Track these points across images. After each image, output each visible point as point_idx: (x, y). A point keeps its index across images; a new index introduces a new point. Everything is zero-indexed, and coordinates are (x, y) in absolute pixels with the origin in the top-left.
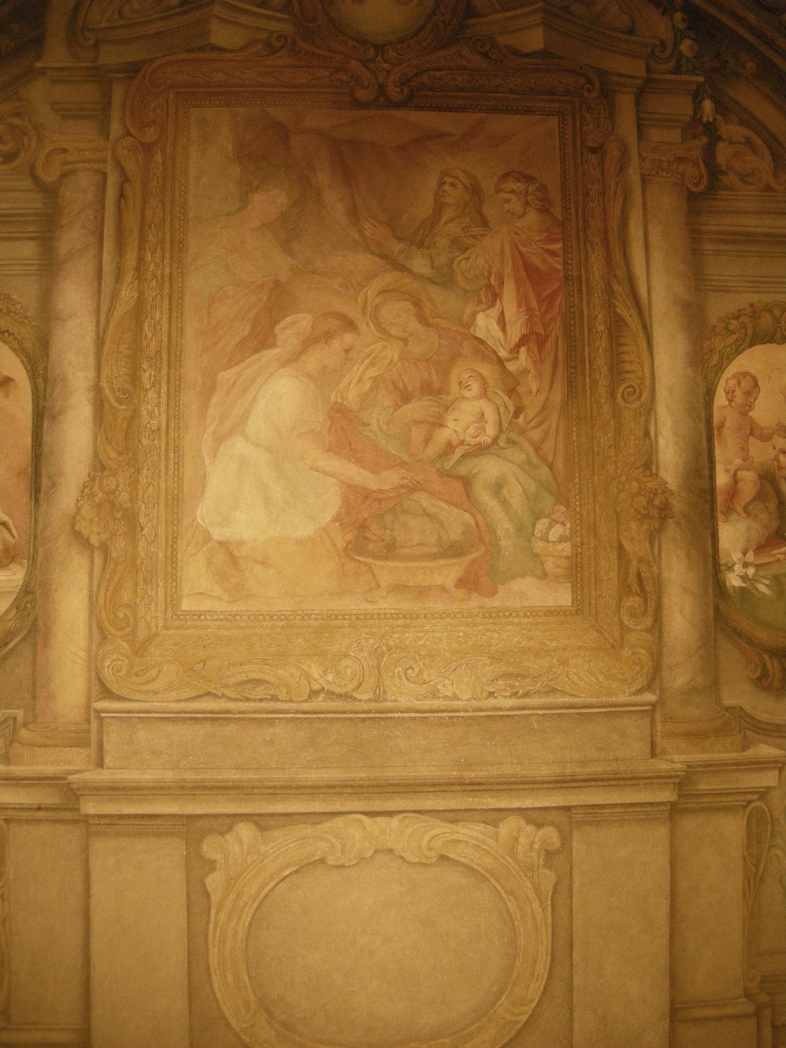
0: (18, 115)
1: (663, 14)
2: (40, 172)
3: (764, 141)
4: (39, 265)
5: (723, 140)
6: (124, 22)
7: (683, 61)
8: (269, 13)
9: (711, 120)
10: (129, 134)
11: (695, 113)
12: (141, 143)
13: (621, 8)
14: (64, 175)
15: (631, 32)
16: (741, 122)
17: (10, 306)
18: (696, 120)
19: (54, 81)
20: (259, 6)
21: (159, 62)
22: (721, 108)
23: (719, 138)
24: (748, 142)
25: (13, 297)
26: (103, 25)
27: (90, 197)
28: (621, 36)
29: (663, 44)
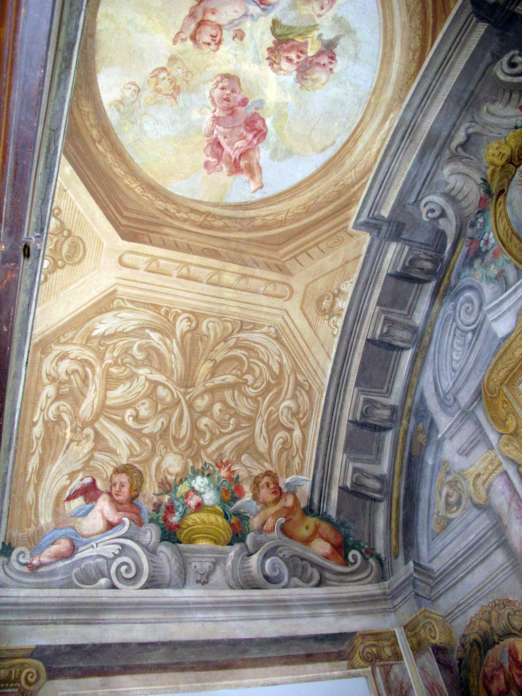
0: (448, 473)
2: (476, 500)
4: (510, 565)
6: (458, 373)
8: (514, 287)
10: (502, 434)
12: (510, 434)
14: (488, 491)
17: (512, 607)
19: (451, 438)
20: (506, 291)
21: (486, 377)
25: (511, 599)
26: (451, 385)
27: (507, 493)
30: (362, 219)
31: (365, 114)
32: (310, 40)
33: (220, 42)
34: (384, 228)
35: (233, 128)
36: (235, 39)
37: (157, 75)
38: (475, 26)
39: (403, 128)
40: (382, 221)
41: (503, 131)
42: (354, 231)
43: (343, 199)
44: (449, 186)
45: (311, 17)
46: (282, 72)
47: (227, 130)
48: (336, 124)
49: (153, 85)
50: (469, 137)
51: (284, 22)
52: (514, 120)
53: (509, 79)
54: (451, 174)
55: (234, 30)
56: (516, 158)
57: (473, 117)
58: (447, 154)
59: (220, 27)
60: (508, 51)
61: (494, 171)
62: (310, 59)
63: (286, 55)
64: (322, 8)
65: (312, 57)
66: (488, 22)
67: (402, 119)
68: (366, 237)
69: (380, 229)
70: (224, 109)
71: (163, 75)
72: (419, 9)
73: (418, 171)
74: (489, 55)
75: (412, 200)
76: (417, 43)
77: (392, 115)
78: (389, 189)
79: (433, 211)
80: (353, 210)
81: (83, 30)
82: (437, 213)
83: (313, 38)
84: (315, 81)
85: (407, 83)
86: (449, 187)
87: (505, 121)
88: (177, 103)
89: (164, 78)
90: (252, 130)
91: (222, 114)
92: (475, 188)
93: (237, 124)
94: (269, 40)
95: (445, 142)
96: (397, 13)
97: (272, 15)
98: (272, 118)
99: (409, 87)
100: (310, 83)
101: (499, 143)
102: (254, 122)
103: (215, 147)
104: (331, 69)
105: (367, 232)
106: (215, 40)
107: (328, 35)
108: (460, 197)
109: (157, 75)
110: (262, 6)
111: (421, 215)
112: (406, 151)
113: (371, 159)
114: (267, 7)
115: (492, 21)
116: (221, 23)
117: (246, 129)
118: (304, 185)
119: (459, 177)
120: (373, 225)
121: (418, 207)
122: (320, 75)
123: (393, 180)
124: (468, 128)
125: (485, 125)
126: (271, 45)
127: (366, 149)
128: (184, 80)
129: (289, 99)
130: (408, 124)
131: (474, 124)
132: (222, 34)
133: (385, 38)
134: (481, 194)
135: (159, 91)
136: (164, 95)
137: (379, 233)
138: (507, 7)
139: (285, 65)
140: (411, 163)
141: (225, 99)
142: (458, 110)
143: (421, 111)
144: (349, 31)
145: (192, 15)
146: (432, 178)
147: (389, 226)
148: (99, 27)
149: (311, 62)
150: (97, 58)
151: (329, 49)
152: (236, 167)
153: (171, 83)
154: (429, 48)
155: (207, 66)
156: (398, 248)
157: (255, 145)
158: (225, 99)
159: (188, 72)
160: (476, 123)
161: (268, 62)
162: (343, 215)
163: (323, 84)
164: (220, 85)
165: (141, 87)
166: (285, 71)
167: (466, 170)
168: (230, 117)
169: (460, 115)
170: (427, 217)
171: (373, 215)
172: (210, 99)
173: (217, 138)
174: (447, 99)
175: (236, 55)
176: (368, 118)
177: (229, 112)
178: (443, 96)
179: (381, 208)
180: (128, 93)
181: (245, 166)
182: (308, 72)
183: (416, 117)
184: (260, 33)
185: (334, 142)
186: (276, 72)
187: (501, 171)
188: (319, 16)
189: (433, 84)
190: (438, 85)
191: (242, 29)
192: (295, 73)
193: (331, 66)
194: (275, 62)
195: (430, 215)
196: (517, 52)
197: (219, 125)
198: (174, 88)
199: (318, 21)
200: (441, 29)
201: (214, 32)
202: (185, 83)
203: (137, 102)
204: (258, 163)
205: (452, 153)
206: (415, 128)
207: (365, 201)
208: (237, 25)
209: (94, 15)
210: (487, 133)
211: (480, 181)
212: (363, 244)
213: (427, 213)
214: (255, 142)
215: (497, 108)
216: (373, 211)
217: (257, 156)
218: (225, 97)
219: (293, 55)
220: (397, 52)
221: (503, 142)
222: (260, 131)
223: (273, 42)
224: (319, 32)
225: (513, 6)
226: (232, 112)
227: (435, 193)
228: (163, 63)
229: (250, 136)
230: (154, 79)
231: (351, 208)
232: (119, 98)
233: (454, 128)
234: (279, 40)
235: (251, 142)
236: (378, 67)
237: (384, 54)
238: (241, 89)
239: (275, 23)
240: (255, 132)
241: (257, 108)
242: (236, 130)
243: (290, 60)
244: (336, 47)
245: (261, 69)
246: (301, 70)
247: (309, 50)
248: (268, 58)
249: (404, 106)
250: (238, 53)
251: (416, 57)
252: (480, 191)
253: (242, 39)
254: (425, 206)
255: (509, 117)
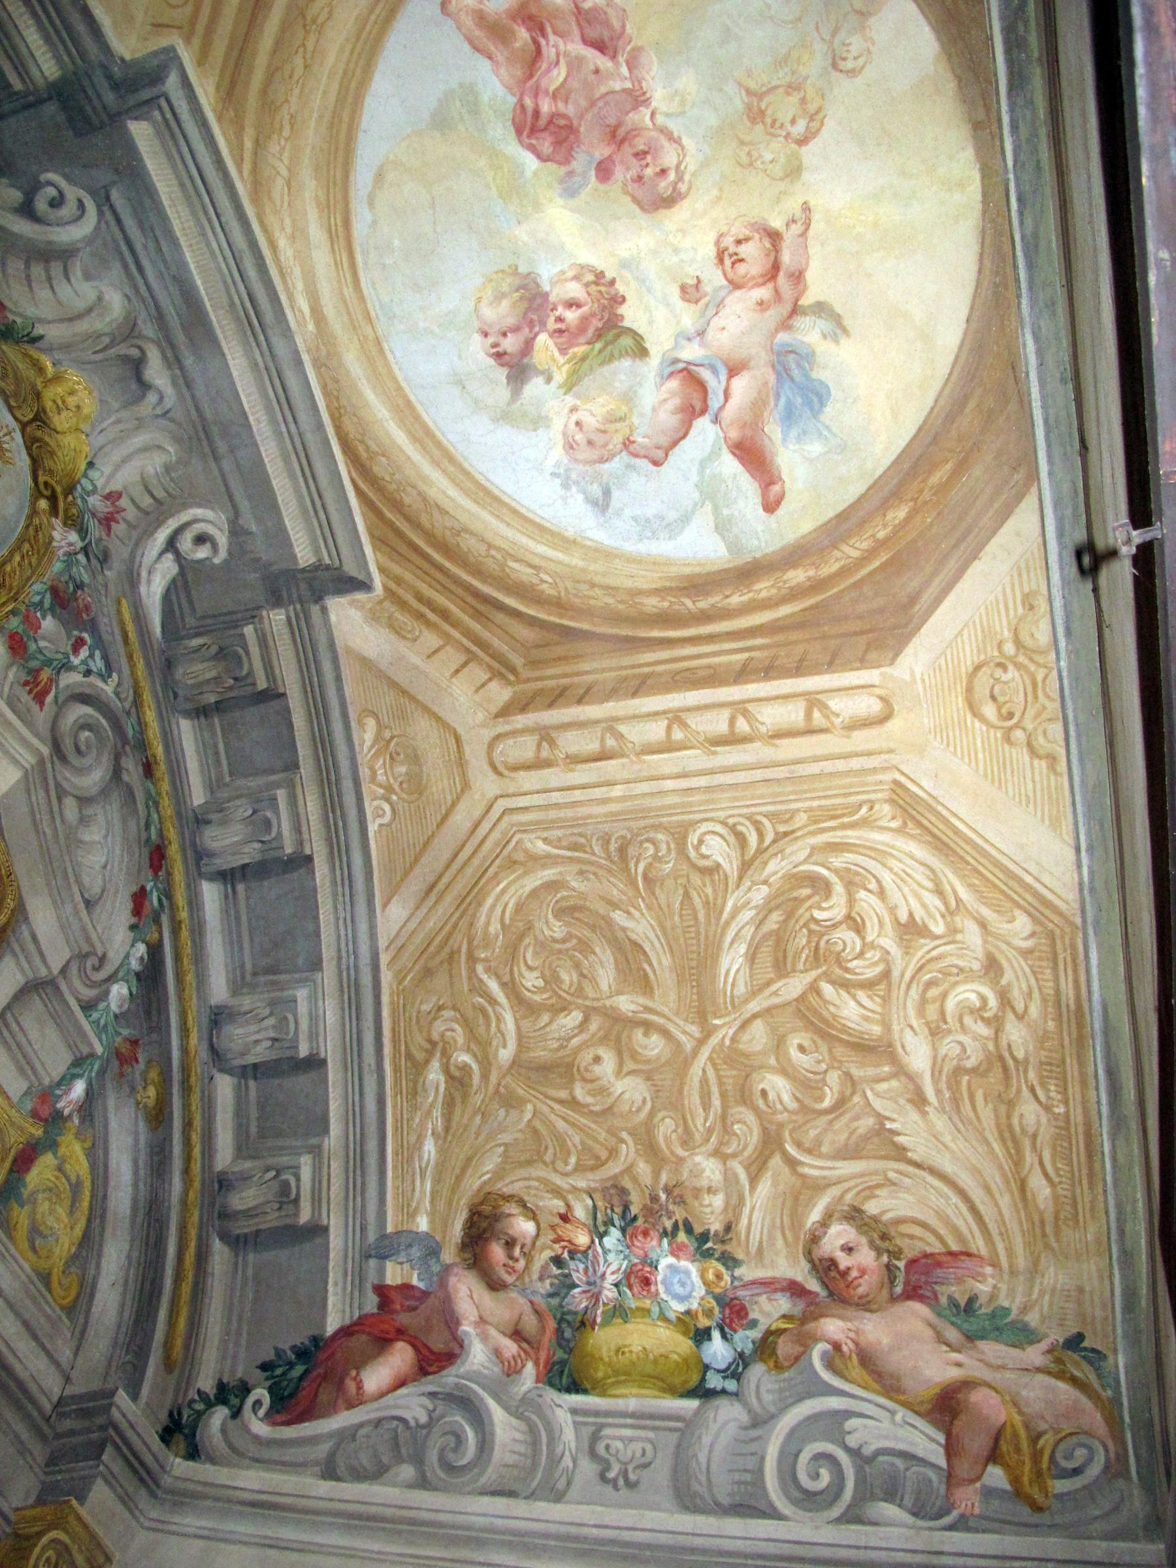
1: (133, 928)
3: (91, 1209)
5: (55, 1154)
7: (102, 1006)
9: (66, 1112)
11: (59, 1084)
13: (105, 867)
15: (88, 904)
16: (90, 1153)
18: (46, 1096)
22: (88, 1108)
23: (53, 1145)
24: (76, 1188)
28: (78, 898)
29: (103, 959)
30: (172, 81)
31: (362, 299)
32: (561, 360)
33: (720, 260)
34: (109, 97)
35: (593, 103)
36: (695, 281)
37: (812, 119)
38: (317, 550)
39: (269, 317)
40: (129, 109)
41: (101, 440)
42: (163, 42)
43: (253, 100)
44: (79, 273)
45: (587, 399)
46: (570, 274)
47: (603, 89)
48: (396, 242)
49: (810, 93)
50: (145, 386)
51: (626, 363)
52: (107, 470)
53: (185, 517)
54: (100, 299)
55: (706, 295)
56: (39, 434)
57: (172, 420)
58: (148, 329)
59: (735, 285)
60: (230, 553)
61: (41, 370)
62: (537, 329)
63: (585, 309)
64: (577, 424)
65: (536, 335)
66: (303, 570)
67: (287, 333)
68: (127, 45)
69: (116, 86)
70: (636, 131)
71: (800, 128)
72: (424, 519)
73: (165, 261)
74: (254, 528)
75: (115, 194)
76: (380, 468)
77: (311, 327)
78: (182, 185)
79: (57, 202)
80: (211, 89)
81: (1000, 128)
82: (41, 205)
83: (559, 368)
84: (500, 297)
85: (338, 398)
86: (77, 272)
87: (116, 457)
88: (740, 84)
89: (793, 122)
90: (550, 122)
91: (633, 118)
92: (31, 311)
93: (589, 116)
94: (632, 315)
95: (173, 347)
96: (452, 492)
97: (654, 361)
98: (529, 174)
99: (326, 394)
100: (505, 288)
101: (88, 417)
102: (558, 144)
103: (606, 35)
104: (486, 335)
105: (135, 62)
106: (731, 256)
107: (535, 387)
108: (37, 270)
109: (812, 119)
110: (681, 366)
111: (66, 177)
112: (225, 282)
113: (271, 219)
114: (670, 369)
115: (300, 576)
116: (738, 293)
117: (564, 116)
118: (358, 72)
119: (80, 305)
120: (142, 84)
121: (93, 193)
122: (500, 313)
123: (194, 213)
124: (161, 398)
125: (140, 424)
126: (623, 310)
127: (298, 234)
128: (751, 143)
129: (522, 234)
130: (270, 332)
131: (159, 411)
132: (725, 275)
133: (438, 444)
134: (14, 313)
135: (791, 88)
136: (776, 88)
137: (109, 77)
138: (298, 606)
139: (575, 290)
140: (192, 266)
141: (646, 153)
142: (208, 414)
143: (267, 369)
144: (504, 417)
145: (798, 277)
146: (125, 266)
147: (105, 108)
148: (969, 153)
149: (531, 324)
150: (951, 86)
151: (517, 367)
152: (531, 18)
153: (774, 121)
154: (354, 475)
155: (719, 198)
156: (34, 72)
157: (522, 95)
158: (646, 153)
159: (751, 164)
160: (157, 416)
161: (609, 275)
162: (220, 61)
163: (479, 300)
164: (672, 176)
165: (835, 75)
166: (566, 280)
167: (83, 326)
168: (612, 121)
169: (198, 409)
170: (50, 183)
171: (160, 108)
172: (676, 135)
173: (614, 57)
174: (247, 418)
175: (676, 251)
176: (348, 292)
177: (621, 132)
178: (258, 421)
179: (158, 133)
180: (856, 43)
181: (513, 32)
182: (525, 305)
183: (267, 353)
184: (656, 316)
185: (371, 204)
186: (582, 267)
187: (33, 386)
188: (574, 409)
189: (292, 427)
190: (284, 429)
191: (693, 307)
192: (546, 287)
193: (491, 340)
194: (596, 283)
195: (51, 192)
196: (217, 561)
197: (624, 90)
198: (762, 113)
199: (570, 400)
200: (363, 515)
201: (742, 269)
202: (747, 138)
203: (828, 38)
204: (490, 58)
205: (140, 336)
206: (249, 333)
207: (204, 125)
208: (707, 306)
209: (986, 173)
210: (124, 414)
211: (39, 330)
212: (115, 24)
213: (61, 194)
214: (528, 102)
215: (154, 464)
216: (169, 116)
217: (503, 71)
218: (649, 158)
219: (571, 316)
220: (400, 437)
221: (85, 427)
222: (534, 131)
223: (622, 317)
224: (554, 384)
225: (292, 614)
226: (617, 136)
227: (90, 240)
228: (809, 153)
229: (546, 107)
230: (812, 108)
231: (217, 89)
232: (872, 21)
233: (184, 381)
234: (616, 326)
235: (536, 96)
236: (407, 390)
237: (417, 418)
238: (627, 193)
239: (641, 351)
240: (542, 122)
241: (571, 174)
242: (584, 103)
243: (572, 304)
244: (509, 378)
245: (613, 255)
246: (539, 301)
247: (550, 342)
248: (612, 282)
249: (305, 357)
250: (675, 259)
251: (361, 449)
252: (21, 315)
253: (683, 289)
254: (81, 205)
255: (117, 468)
